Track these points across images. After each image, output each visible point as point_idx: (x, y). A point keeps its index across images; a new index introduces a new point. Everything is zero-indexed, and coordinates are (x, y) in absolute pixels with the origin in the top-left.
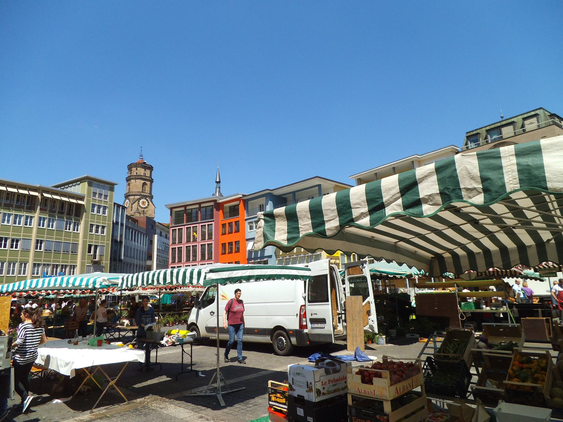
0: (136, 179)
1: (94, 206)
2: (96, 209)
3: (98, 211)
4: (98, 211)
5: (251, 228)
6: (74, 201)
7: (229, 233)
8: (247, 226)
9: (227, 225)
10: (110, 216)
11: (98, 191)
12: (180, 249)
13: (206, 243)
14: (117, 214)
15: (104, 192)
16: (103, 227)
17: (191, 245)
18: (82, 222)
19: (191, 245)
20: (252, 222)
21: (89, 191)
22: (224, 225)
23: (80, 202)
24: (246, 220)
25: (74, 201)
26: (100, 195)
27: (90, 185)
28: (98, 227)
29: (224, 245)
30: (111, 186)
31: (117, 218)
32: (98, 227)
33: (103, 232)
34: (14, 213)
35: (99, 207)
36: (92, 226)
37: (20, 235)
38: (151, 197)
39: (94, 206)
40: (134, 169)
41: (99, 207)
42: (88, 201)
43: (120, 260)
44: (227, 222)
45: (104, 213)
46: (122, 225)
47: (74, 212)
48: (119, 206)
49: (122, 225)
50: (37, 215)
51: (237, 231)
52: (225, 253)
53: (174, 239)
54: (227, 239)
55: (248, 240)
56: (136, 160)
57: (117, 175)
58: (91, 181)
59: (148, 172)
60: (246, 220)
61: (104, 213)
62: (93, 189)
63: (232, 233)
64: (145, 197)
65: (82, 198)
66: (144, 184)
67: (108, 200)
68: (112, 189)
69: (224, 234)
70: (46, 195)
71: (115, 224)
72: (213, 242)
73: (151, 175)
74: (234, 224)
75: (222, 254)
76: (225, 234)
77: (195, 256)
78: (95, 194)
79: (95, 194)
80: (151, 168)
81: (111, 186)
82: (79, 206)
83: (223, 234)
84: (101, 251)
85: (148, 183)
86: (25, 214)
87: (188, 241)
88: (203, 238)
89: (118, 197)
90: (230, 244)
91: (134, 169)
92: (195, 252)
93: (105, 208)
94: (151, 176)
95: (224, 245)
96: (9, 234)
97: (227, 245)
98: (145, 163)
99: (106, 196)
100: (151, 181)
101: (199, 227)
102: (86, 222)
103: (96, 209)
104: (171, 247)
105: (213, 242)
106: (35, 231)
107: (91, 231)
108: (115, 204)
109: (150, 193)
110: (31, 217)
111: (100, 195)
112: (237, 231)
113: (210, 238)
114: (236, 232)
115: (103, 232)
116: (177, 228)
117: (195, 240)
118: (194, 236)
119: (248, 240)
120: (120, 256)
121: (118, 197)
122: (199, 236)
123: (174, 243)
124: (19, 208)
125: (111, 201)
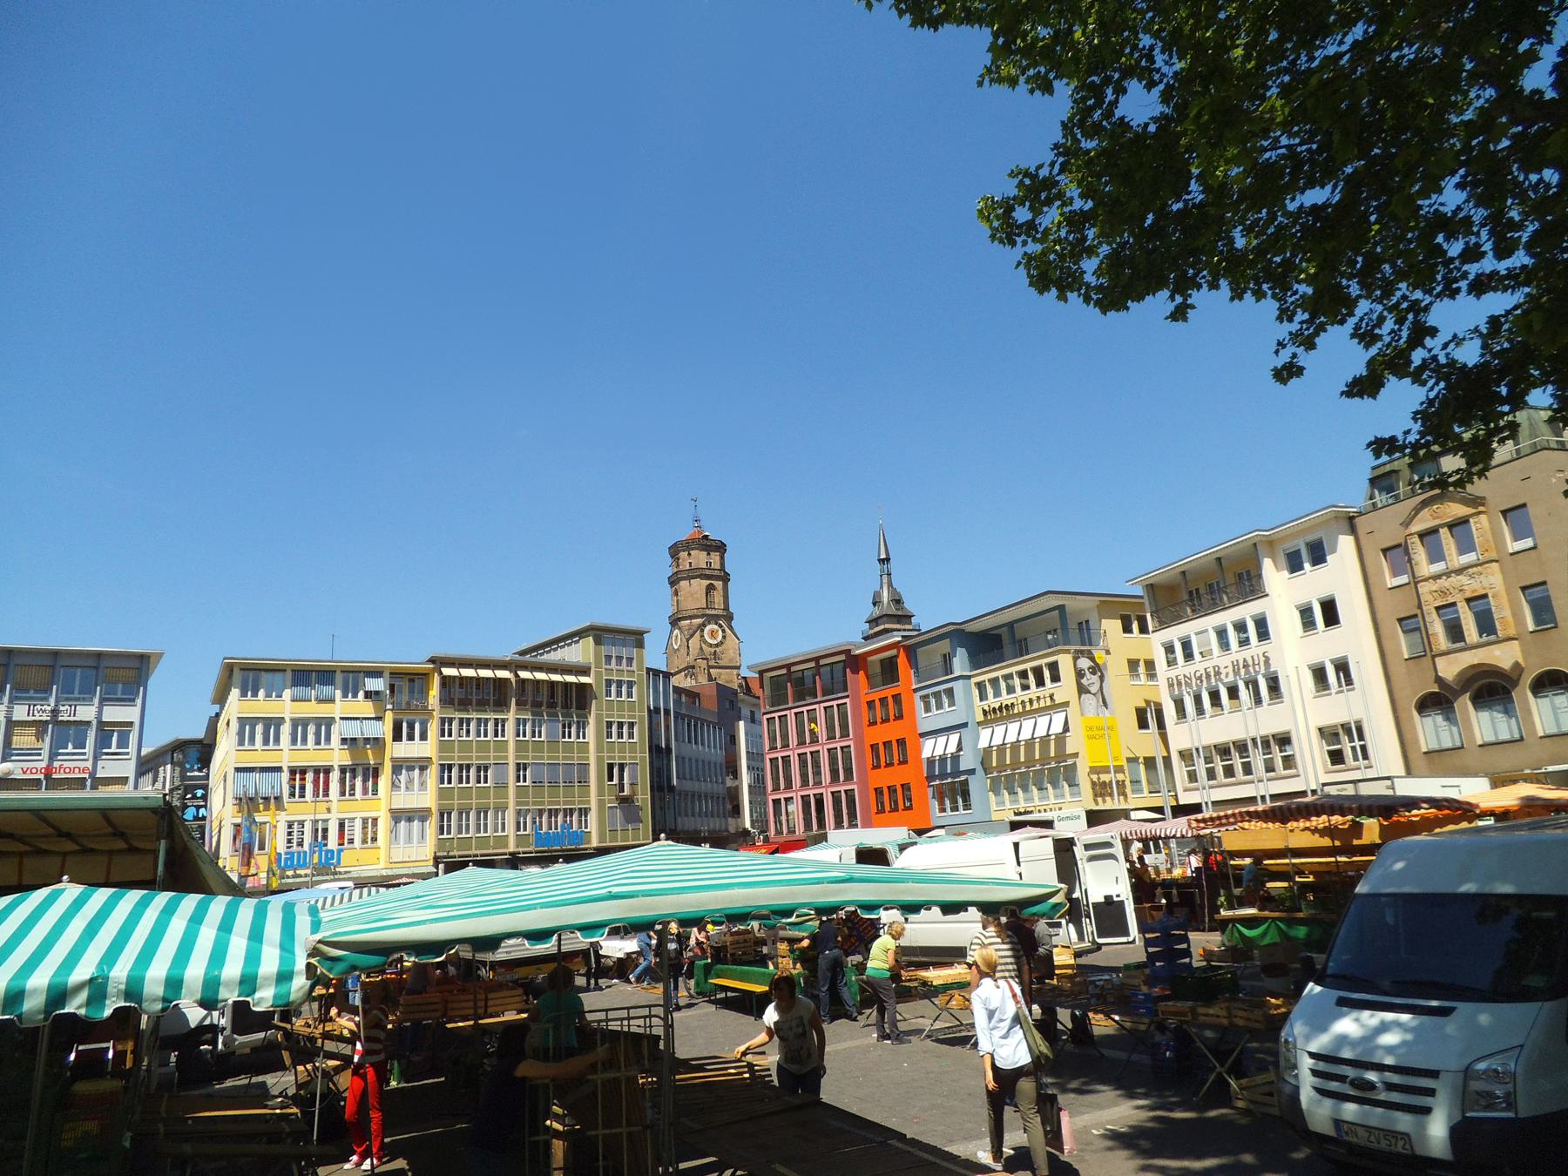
0: (689, 578)
1: (609, 683)
2: (613, 688)
3: (619, 694)
4: (619, 694)
5: (928, 709)
6: (571, 679)
7: (883, 721)
8: (920, 705)
9: (877, 703)
10: (641, 697)
11: (614, 652)
12: (786, 760)
13: (838, 745)
14: (656, 691)
15: (624, 652)
16: (631, 725)
17: (808, 750)
18: (592, 720)
19: (808, 750)
20: (927, 696)
21: (597, 655)
22: (871, 704)
23: (584, 679)
24: (915, 691)
25: (571, 679)
26: (619, 659)
27: (598, 642)
28: (620, 725)
29: (874, 747)
30: (637, 638)
31: (656, 699)
32: (620, 725)
33: (631, 735)
34: (474, 715)
35: (619, 684)
36: (610, 725)
37: (488, 758)
38: (729, 618)
39: (609, 683)
40: (683, 555)
41: (619, 684)
42: (598, 674)
43: (671, 789)
44: (876, 697)
45: (630, 695)
46: (667, 712)
47: (570, 701)
48: (656, 673)
49: (667, 712)
50: (511, 716)
51: (899, 717)
52: (878, 767)
53: (773, 739)
54: (881, 734)
55: (922, 735)
56: (685, 533)
57: (646, 604)
58: (600, 634)
59: (715, 558)
60: (915, 691)
61: (630, 695)
62: (604, 650)
63: (888, 720)
64: (714, 619)
65: (585, 671)
66: (710, 588)
67: (634, 667)
68: (640, 644)
69: (872, 724)
70: (524, 675)
71: (653, 713)
72: (851, 743)
73: (722, 564)
74: (890, 700)
75: (874, 768)
76: (875, 723)
77: (817, 773)
78: (609, 658)
79: (609, 658)
80: (720, 548)
81: (637, 638)
82: (582, 687)
83: (871, 724)
84: (633, 776)
85: (719, 584)
86: (493, 716)
87: (801, 743)
88: (831, 737)
89: (653, 656)
90: (887, 744)
91: (683, 555)
92: (816, 765)
93: (630, 684)
94: (722, 568)
95: (874, 747)
96: (470, 758)
97: (881, 747)
98: (706, 537)
99: (630, 660)
100: (725, 578)
101: (820, 710)
102: (599, 718)
103: (613, 688)
104: (768, 757)
105: (851, 743)
106: (511, 746)
107: (609, 735)
108: (649, 670)
109: (726, 608)
110: (504, 721)
111: (619, 659)
112: (899, 717)
113: (845, 734)
114: (896, 719)
115: (631, 735)
116: (776, 715)
117: (815, 740)
118: (812, 732)
119: (922, 735)
120: (669, 778)
121: (653, 656)
122: (821, 729)
123: (773, 748)
124: (482, 705)
125: (640, 668)
